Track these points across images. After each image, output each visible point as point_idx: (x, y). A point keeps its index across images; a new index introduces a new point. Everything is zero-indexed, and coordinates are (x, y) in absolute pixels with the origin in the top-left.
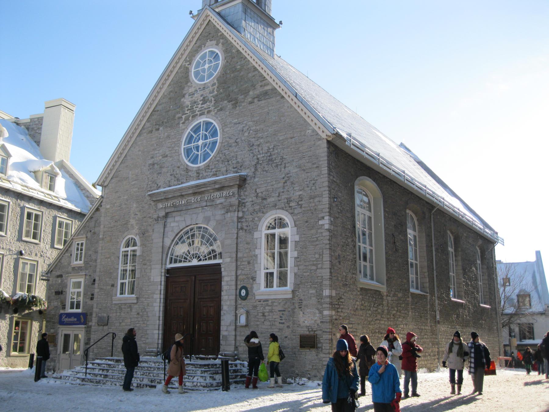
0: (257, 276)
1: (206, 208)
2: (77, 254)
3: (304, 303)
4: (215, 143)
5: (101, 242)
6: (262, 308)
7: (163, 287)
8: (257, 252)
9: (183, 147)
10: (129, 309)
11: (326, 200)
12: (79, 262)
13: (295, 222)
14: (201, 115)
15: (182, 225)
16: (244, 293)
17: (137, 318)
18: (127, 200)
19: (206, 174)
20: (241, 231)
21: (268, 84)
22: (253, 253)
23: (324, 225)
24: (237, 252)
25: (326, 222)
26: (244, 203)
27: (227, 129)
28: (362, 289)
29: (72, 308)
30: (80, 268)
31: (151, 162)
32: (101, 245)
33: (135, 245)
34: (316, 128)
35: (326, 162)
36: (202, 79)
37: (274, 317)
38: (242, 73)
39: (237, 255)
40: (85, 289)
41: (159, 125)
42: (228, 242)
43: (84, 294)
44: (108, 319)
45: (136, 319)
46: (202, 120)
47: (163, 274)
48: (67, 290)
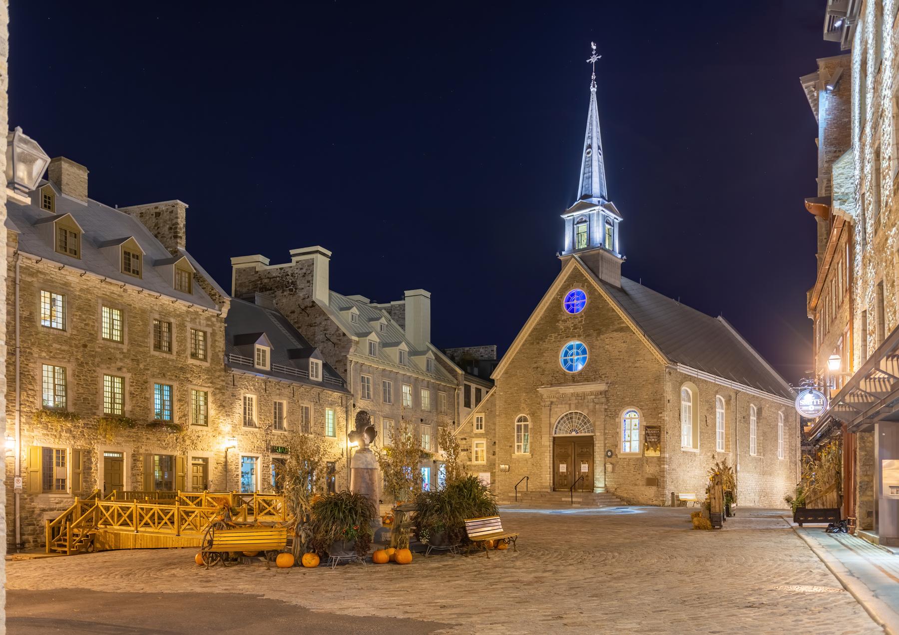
31: (535, 366)
33: (526, 420)
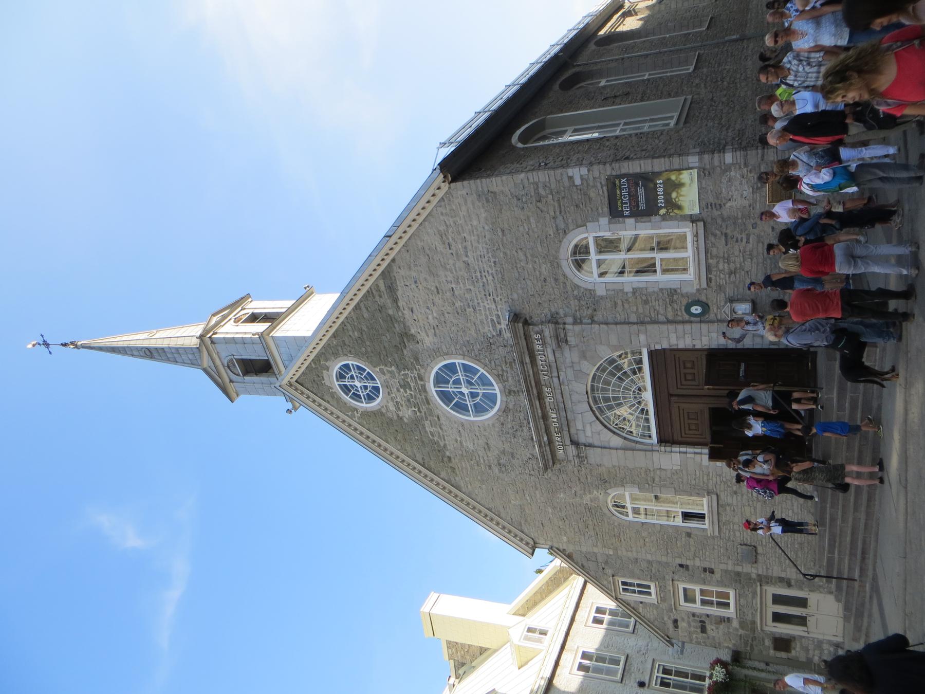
0: (668, 287)
1: (561, 378)
2: (640, 592)
3: (711, 199)
4: (466, 368)
5: (620, 553)
6: (722, 276)
7: (690, 450)
8: (628, 289)
9: (472, 418)
10: (728, 508)
11: (542, 176)
12: (653, 590)
13: (578, 226)
14: (425, 391)
15: (590, 416)
16: (696, 307)
17: (742, 495)
18: (554, 508)
19: (510, 379)
20: (596, 319)
21: (376, 284)
22: (630, 295)
23: (581, 176)
24: (629, 323)
25: (577, 173)
26: (552, 316)
27: (444, 347)
28: (685, 122)
29: (727, 605)
30: (661, 589)
32: (625, 553)
34: (435, 201)
35: (484, 180)
37: (737, 253)
38: (364, 328)
39: (634, 323)
40: (696, 582)
41: (443, 456)
42: (614, 340)
43: (704, 583)
44: (746, 545)
45: (745, 496)
46: (432, 389)
47: (668, 449)
48: (697, 611)
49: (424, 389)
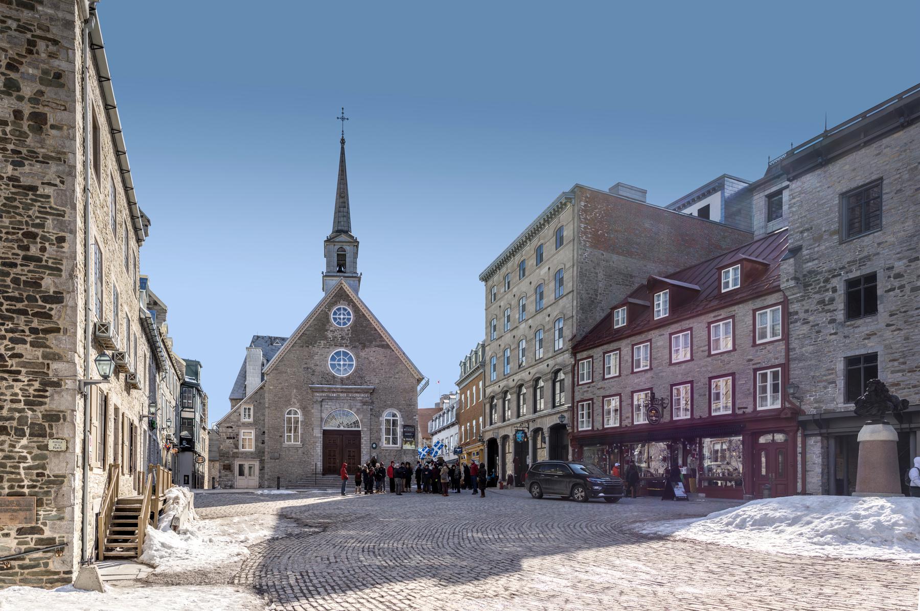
16: (375, 445)
21: (384, 341)
36: (339, 323)
49: (341, 346)
